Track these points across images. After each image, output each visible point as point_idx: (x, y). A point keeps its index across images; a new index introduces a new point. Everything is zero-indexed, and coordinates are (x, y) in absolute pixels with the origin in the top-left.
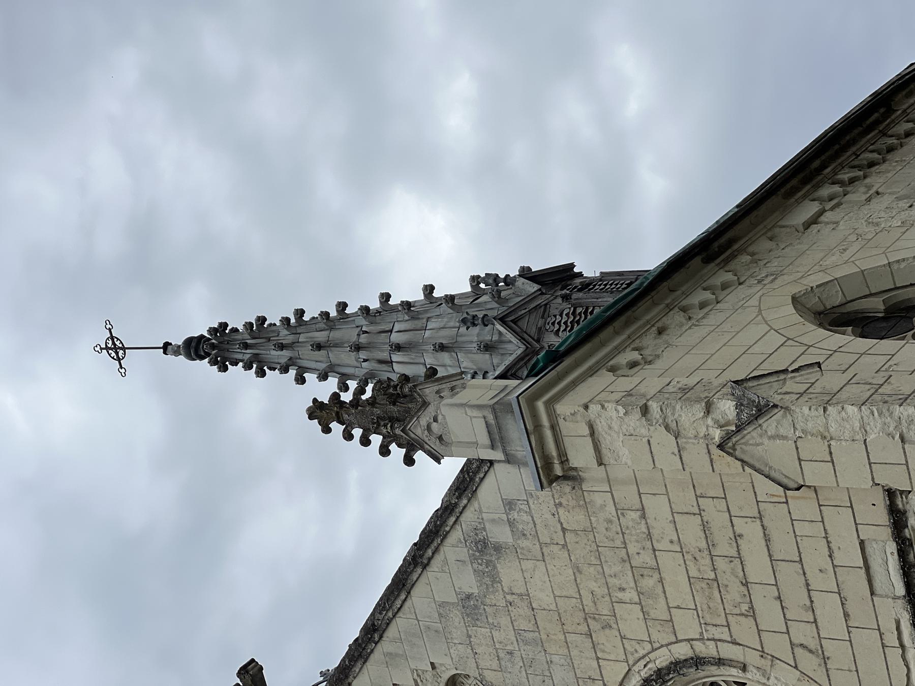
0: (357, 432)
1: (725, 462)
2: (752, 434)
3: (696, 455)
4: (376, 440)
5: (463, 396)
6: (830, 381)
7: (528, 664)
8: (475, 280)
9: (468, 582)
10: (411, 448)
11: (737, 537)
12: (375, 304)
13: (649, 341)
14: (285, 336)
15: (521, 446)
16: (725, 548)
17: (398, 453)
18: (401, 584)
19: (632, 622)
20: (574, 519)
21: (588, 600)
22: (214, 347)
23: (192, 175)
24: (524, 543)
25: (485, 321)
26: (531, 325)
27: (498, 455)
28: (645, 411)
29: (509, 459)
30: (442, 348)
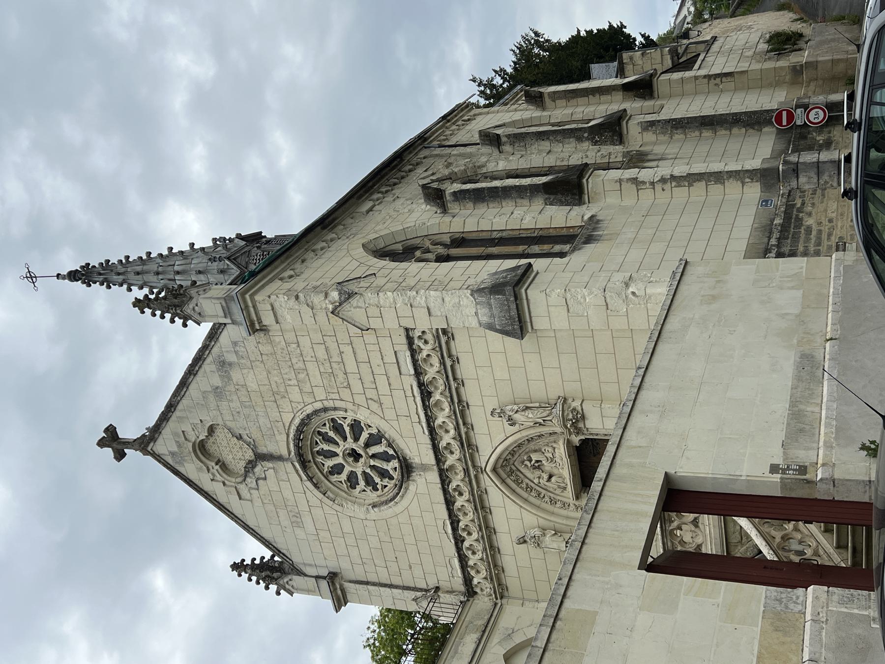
0: (158, 313)
2: (346, 306)
3: (322, 317)
4: (168, 316)
6: (380, 281)
7: (247, 417)
8: (215, 240)
9: (216, 381)
10: (185, 319)
11: (341, 353)
12: (165, 252)
13: (298, 266)
14: (120, 269)
15: (239, 316)
16: (336, 358)
17: (179, 321)
18: (184, 384)
19: (295, 394)
20: (266, 349)
21: (274, 386)
22: (84, 275)
23: (61, 192)
24: (243, 361)
25: (220, 259)
26: (242, 260)
27: (228, 321)
28: (297, 297)
29: (234, 322)
30: (200, 272)
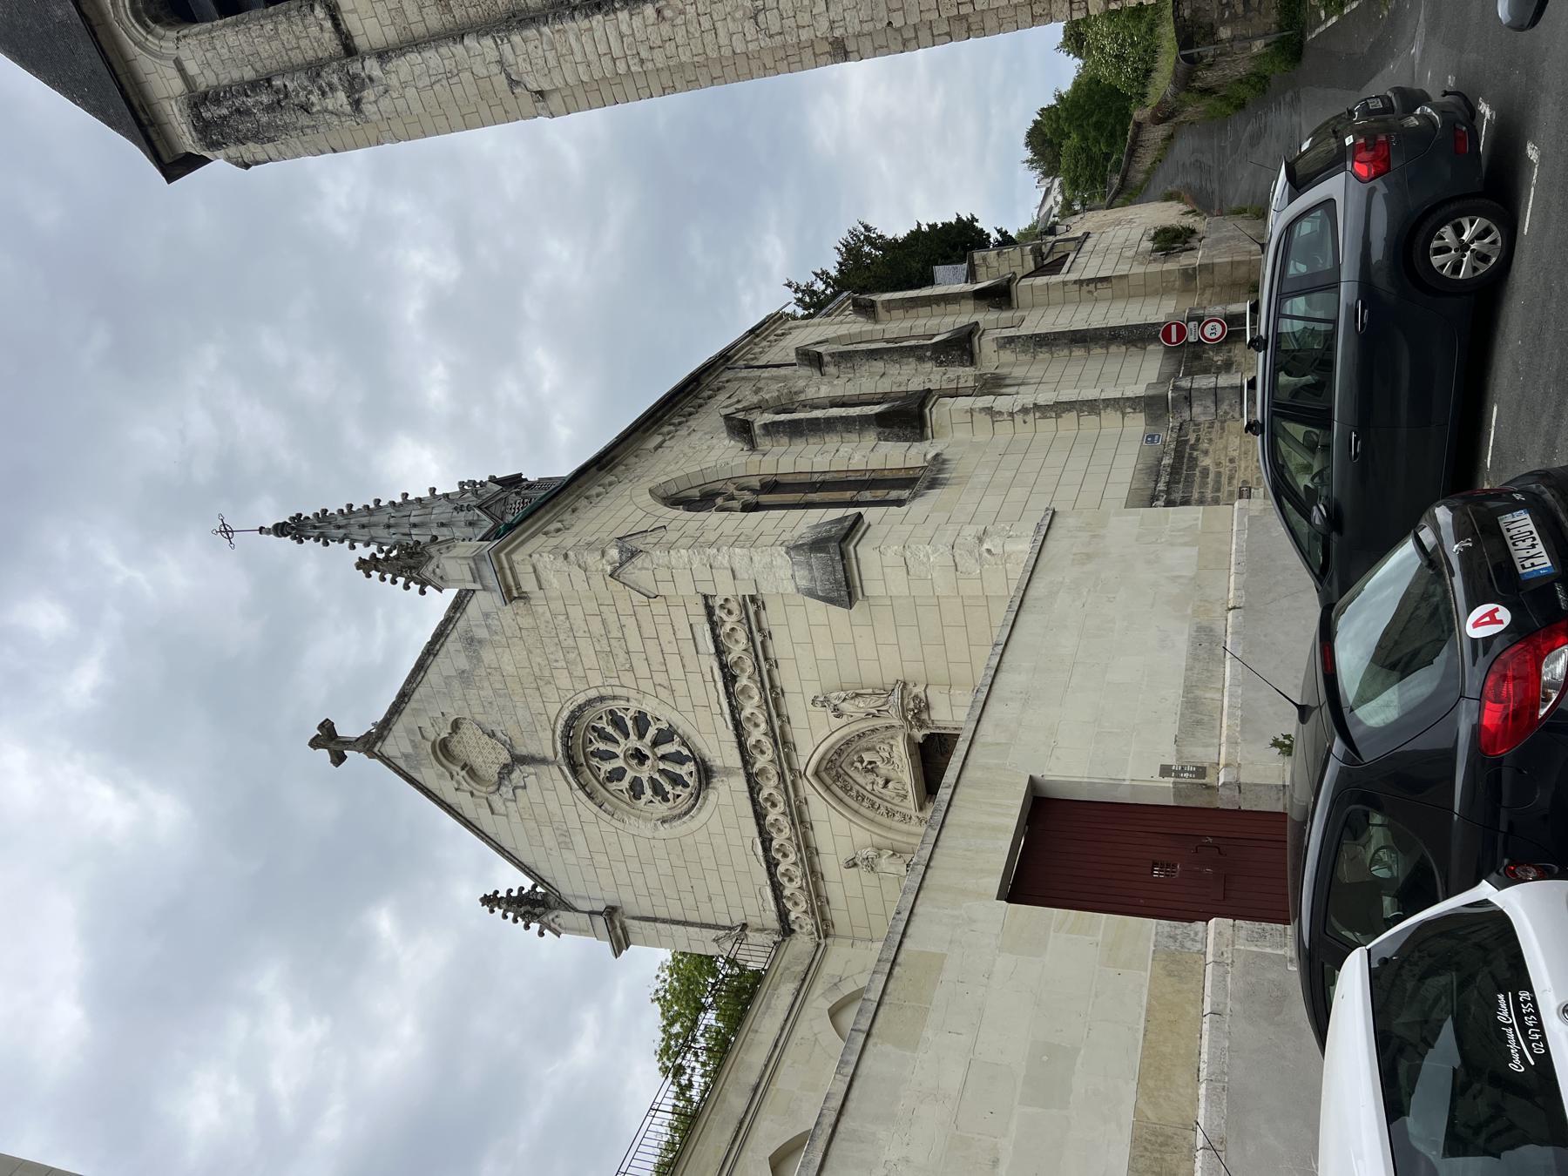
0: (389, 576)
1: (613, 583)
2: (628, 567)
3: (597, 581)
4: (401, 580)
5: (454, 552)
6: (671, 536)
7: (502, 709)
8: (462, 484)
9: (462, 662)
10: (423, 584)
11: (622, 627)
12: (399, 500)
13: (567, 516)
14: (341, 521)
15: (491, 580)
16: (615, 633)
17: (415, 587)
18: (421, 667)
19: (563, 680)
20: (526, 622)
21: (536, 669)
22: (294, 529)
23: (259, 426)
24: (496, 638)
25: (469, 508)
26: (497, 509)
27: (478, 586)
28: (566, 556)
29: (485, 588)
30: (443, 525)
